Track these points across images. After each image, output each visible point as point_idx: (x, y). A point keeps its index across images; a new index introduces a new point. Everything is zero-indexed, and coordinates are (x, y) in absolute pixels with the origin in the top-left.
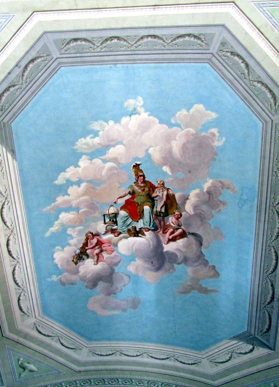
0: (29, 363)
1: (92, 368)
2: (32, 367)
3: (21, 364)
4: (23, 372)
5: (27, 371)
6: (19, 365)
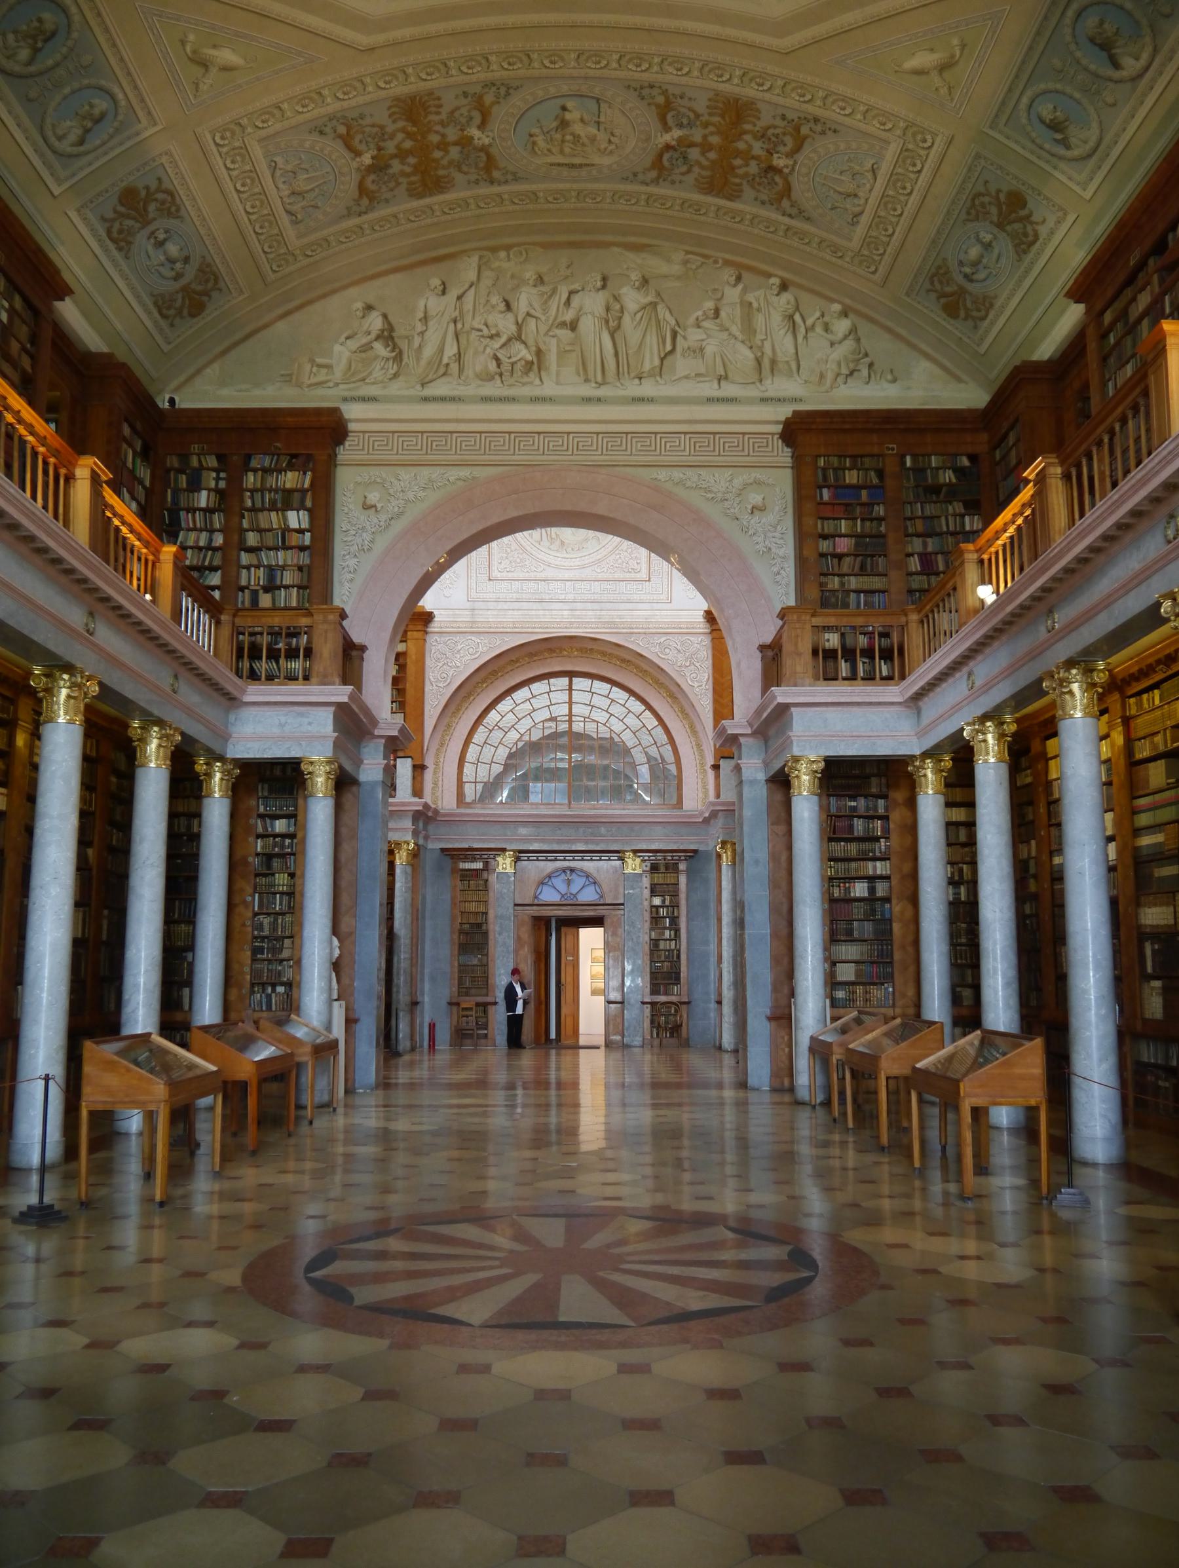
0: (215, 47)
1: (407, 32)
2: (227, 56)
3: (194, 52)
4: (204, 75)
5: (214, 71)
6: (189, 59)
